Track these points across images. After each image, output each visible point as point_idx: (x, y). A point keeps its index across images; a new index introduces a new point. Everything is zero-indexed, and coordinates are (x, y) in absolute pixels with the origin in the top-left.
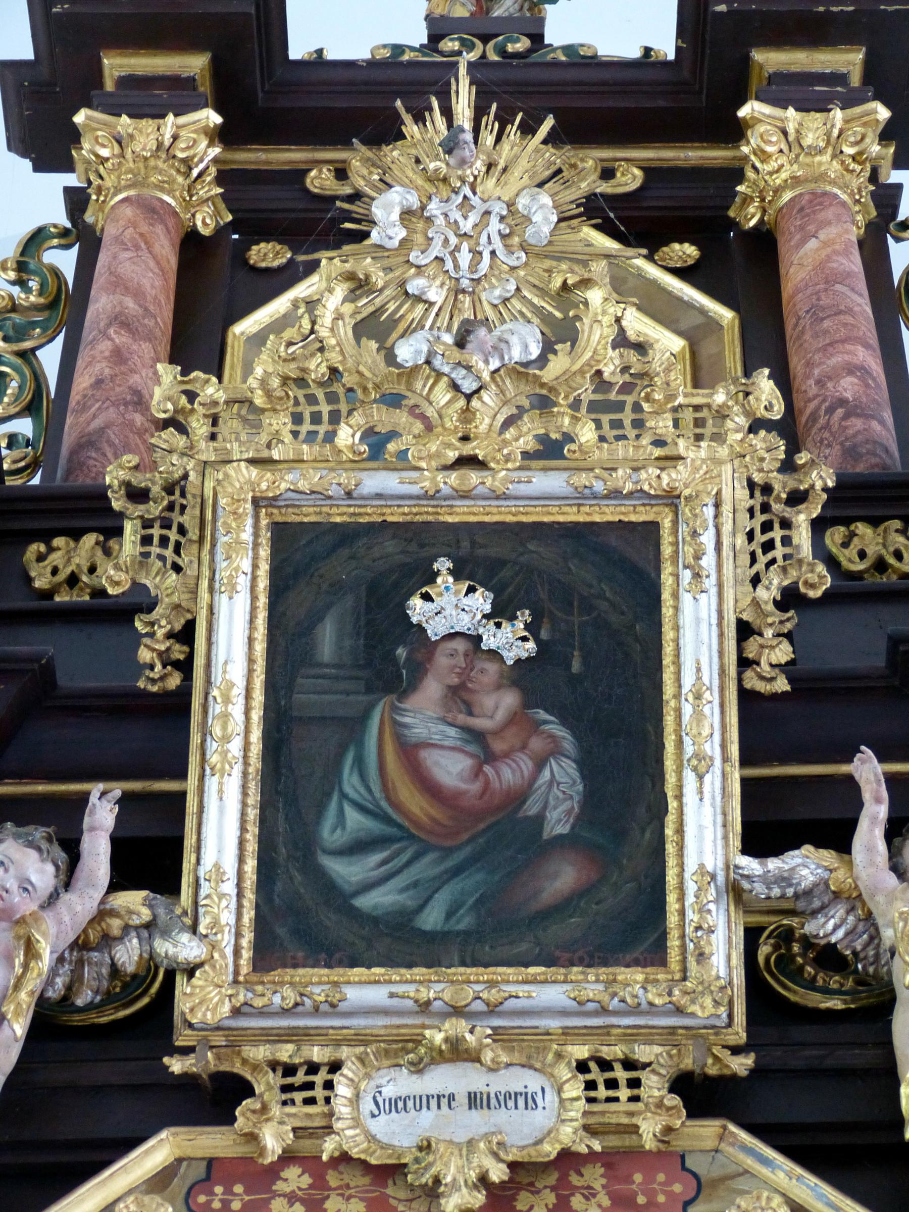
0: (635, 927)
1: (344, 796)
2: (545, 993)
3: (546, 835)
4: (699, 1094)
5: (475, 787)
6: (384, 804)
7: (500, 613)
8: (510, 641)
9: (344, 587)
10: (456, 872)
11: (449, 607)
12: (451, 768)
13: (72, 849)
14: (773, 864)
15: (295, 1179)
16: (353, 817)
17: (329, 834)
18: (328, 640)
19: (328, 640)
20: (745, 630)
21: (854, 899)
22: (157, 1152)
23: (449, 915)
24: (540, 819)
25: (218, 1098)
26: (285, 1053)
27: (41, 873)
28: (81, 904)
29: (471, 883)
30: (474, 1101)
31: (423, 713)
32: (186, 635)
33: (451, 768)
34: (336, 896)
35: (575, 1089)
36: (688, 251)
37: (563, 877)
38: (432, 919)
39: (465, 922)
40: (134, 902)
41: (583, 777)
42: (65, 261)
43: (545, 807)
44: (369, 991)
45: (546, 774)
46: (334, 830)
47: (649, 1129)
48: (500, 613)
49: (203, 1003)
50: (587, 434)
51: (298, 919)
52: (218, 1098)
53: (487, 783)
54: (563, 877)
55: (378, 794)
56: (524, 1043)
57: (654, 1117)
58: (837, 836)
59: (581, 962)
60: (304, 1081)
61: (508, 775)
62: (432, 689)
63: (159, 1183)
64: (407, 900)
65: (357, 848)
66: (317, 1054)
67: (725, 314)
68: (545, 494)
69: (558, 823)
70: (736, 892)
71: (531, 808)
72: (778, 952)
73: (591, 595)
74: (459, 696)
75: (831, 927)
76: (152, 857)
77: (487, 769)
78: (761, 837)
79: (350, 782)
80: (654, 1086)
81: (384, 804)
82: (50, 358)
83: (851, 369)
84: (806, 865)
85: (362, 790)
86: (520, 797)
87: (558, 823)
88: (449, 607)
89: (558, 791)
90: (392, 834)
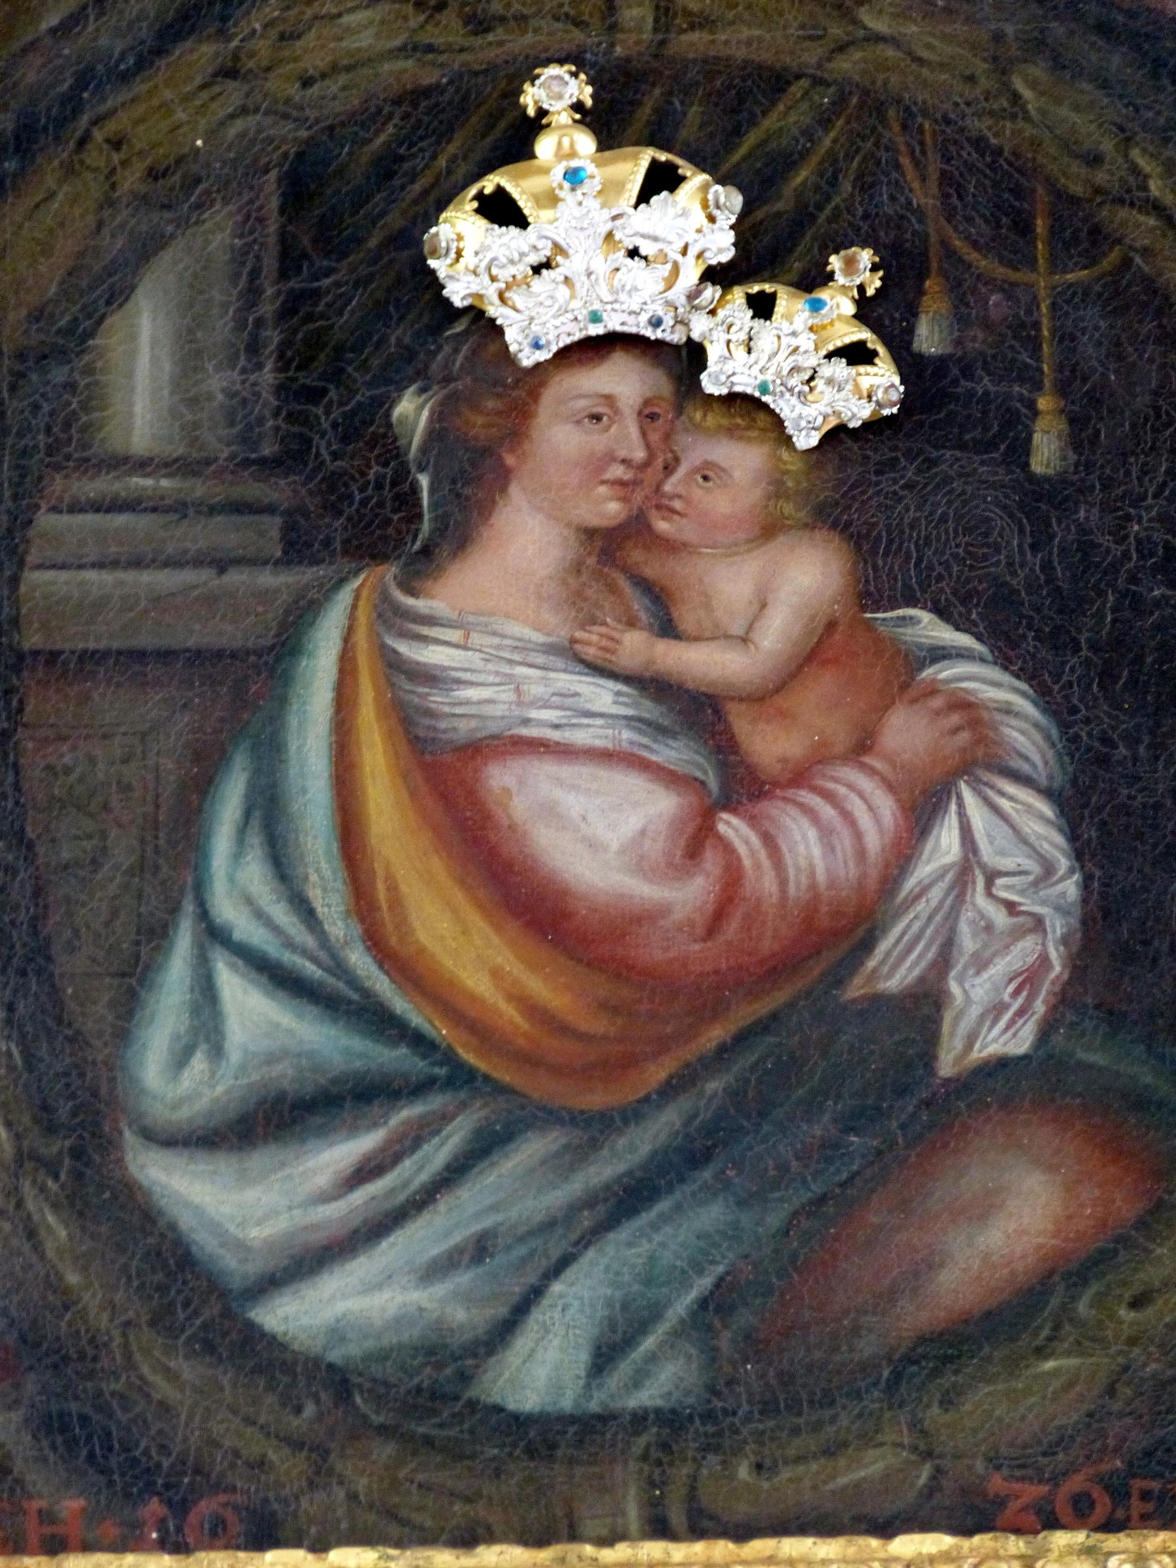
1: (214, 934)
3: (947, 1065)
5: (690, 895)
6: (359, 960)
7: (766, 262)
10: (629, 1199)
12: (600, 828)
16: (247, 1006)
17: (165, 1073)
23: (604, 1358)
24: (925, 1005)
29: (685, 1236)
31: (496, 633)
33: (600, 828)
37: (1012, 1212)
38: (541, 1371)
39: (663, 1379)
41: (1079, 855)
43: (943, 962)
45: (945, 842)
46: (181, 1059)
48: (766, 262)
53: (732, 878)
55: (338, 924)
59: (1080, 1513)
61: (809, 847)
62: (524, 544)
64: (450, 1303)
65: (273, 1119)
69: (991, 1015)
71: (894, 966)
74: (626, 563)
77: (731, 826)
79: (235, 882)
81: (359, 960)
85: (281, 914)
86: (848, 926)
87: (991, 1015)
90: (396, 1069)
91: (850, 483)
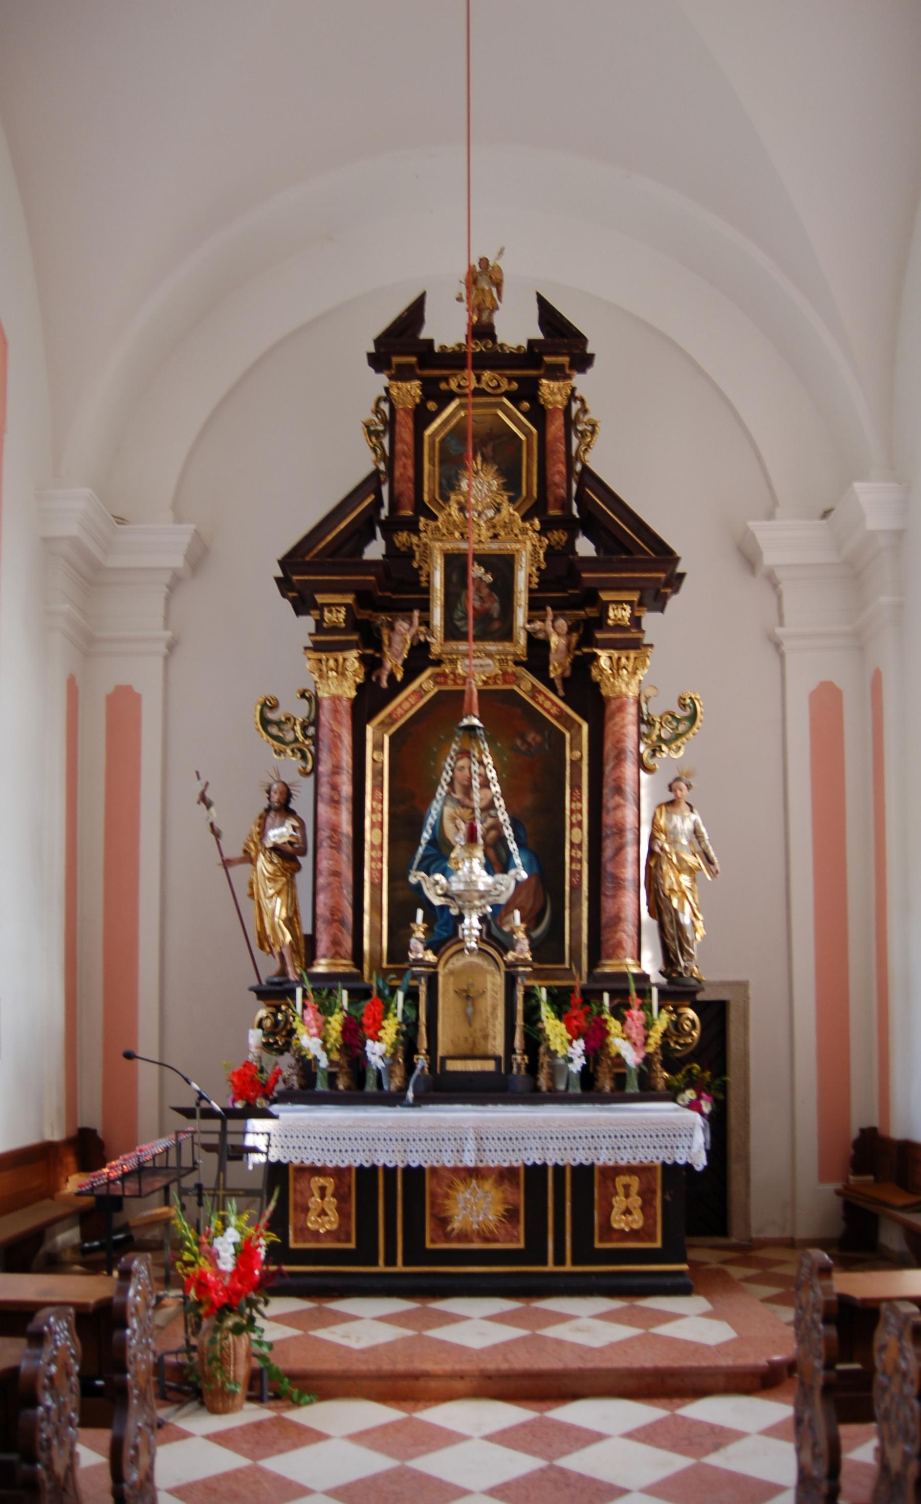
0: (507, 634)
2: (492, 647)
4: (517, 663)
7: (486, 572)
8: (489, 578)
9: (456, 564)
11: (476, 571)
13: (411, 624)
14: (532, 626)
15: (452, 676)
17: (456, 616)
18: (455, 578)
19: (455, 578)
20: (530, 576)
21: (545, 631)
22: (429, 672)
25: (438, 662)
26: (450, 657)
27: (406, 626)
28: (413, 631)
30: (481, 666)
32: (428, 576)
34: (457, 628)
35: (497, 664)
36: (526, 405)
37: (496, 625)
40: (423, 629)
42: (385, 407)
44: (462, 646)
47: (510, 670)
49: (436, 649)
50: (502, 533)
51: (453, 632)
52: (438, 662)
54: (496, 625)
56: (489, 655)
57: (511, 668)
58: (544, 621)
60: (453, 662)
61: (487, 605)
63: (429, 678)
66: (455, 657)
67: (534, 430)
68: (494, 547)
69: (495, 615)
70: (525, 628)
72: (530, 636)
73: (501, 567)
74: (478, 590)
75: (541, 636)
76: (426, 622)
78: (530, 621)
79: (459, 606)
80: (510, 663)
82: (386, 442)
83: (559, 472)
84: (538, 625)
87: (495, 614)
88: (476, 571)
89: (495, 608)
91: (491, 586)
